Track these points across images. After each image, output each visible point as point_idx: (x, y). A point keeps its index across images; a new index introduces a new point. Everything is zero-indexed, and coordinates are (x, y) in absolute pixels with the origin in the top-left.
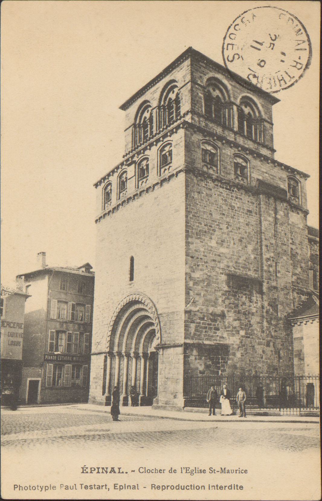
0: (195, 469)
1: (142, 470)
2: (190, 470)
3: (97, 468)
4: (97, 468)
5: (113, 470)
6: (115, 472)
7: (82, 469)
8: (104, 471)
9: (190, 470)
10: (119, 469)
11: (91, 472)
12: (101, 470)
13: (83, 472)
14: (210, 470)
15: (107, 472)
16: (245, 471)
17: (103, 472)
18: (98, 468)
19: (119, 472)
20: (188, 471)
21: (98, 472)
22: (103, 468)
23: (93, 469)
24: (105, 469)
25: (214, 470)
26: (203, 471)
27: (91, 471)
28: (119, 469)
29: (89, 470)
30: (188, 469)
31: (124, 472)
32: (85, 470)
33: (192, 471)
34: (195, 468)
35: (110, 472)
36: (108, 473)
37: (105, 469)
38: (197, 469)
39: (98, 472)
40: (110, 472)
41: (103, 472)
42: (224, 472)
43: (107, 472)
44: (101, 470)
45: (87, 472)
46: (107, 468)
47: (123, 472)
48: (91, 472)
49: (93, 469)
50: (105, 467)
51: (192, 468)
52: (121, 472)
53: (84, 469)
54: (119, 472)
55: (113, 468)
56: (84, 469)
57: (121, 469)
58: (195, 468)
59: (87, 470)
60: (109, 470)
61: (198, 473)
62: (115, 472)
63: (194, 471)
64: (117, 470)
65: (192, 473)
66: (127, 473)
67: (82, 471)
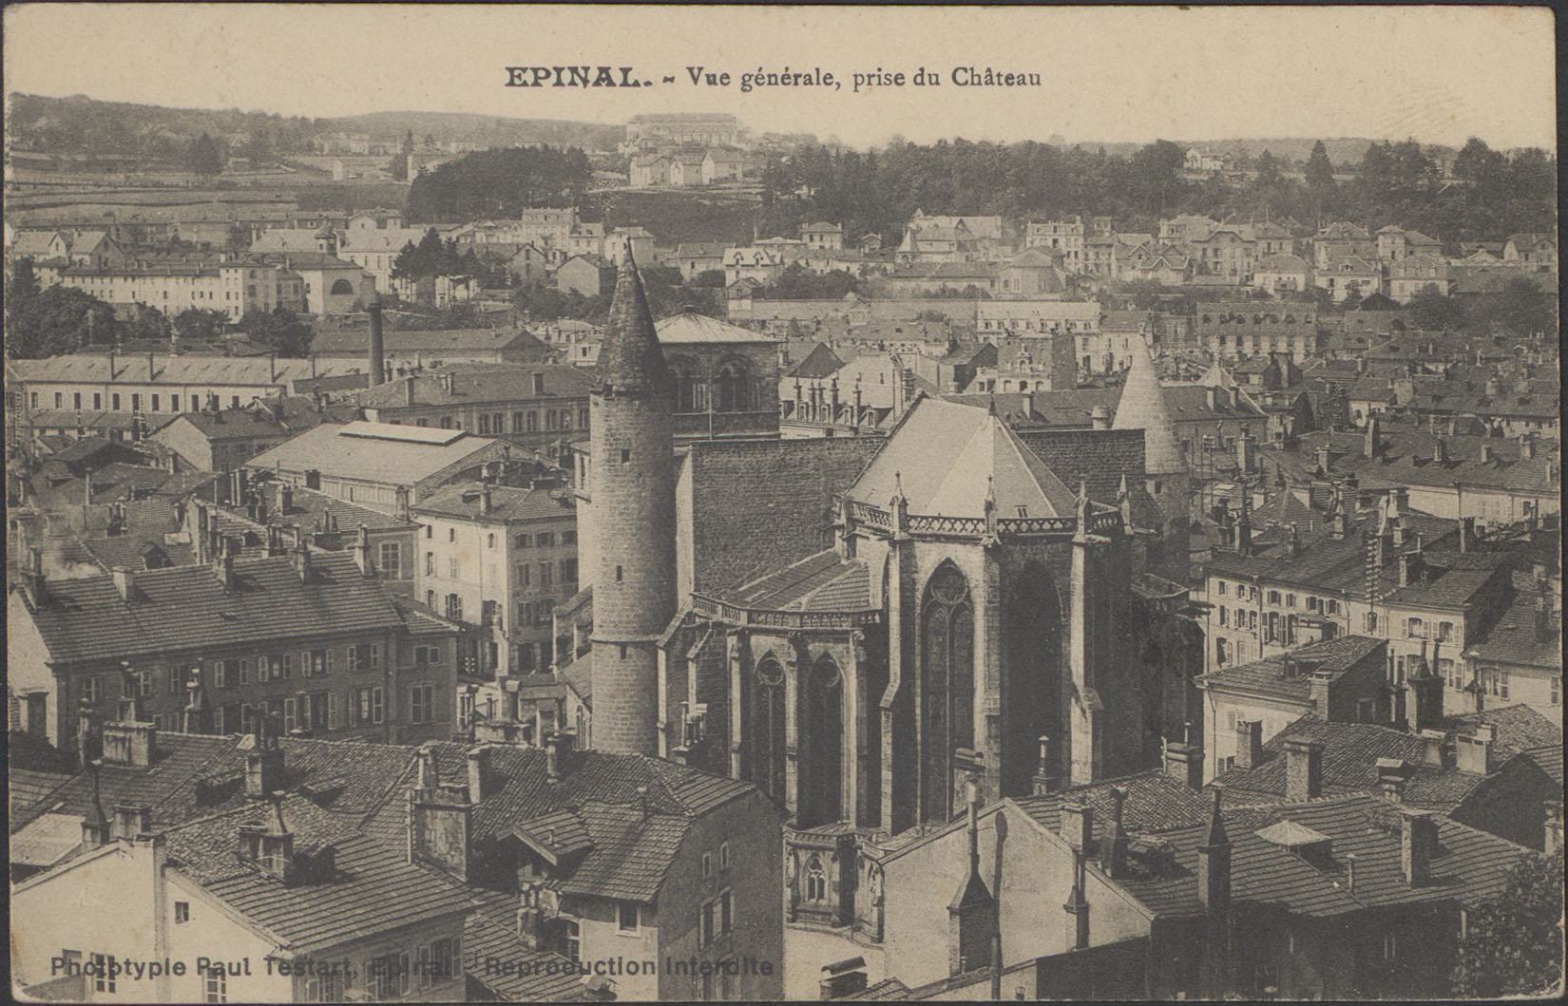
3: (555, 69)
4: (555, 69)
5: (605, 77)
6: (611, 83)
7: (508, 74)
8: (577, 80)
10: (625, 71)
12: (566, 76)
13: (511, 84)
15: (585, 82)
18: (559, 70)
19: (625, 84)
21: (559, 83)
22: (574, 70)
23: (542, 74)
24: (582, 73)
27: (537, 78)
28: (625, 71)
29: (529, 77)
31: (641, 83)
32: (519, 76)
35: (597, 84)
36: (590, 85)
37: (582, 73)
39: (559, 83)
40: (597, 84)
41: (573, 83)
43: (585, 82)
44: (566, 76)
45: (525, 84)
46: (586, 69)
47: (636, 84)
48: (536, 84)
49: (542, 74)
50: (579, 64)
52: (631, 81)
53: (516, 73)
55: (602, 70)
56: (516, 73)
57: (630, 74)
59: (524, 77)
60: (593, 75)
62: (611, 83)
64: (617, 77)
66: (648, 84)
67: (508, 80)
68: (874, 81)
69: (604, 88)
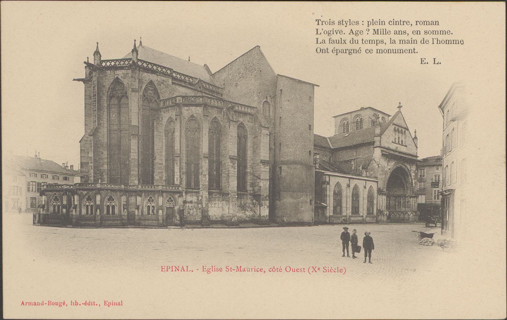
0: (211, 267)
1: (288, 269)
2: (207, 268)
6: (184, 271)
9: (207, 268)
11: (167, 271)
14: (324, 269)
15: (178, 270)
16: (260, 269)
17: (175, 271)
19: (187, 271)
20: (205, 270)
23: (168, 268)
25: (231, 268)
26: (220, 269)
30: (205, 267)
33: (209, 269)
34: (212, 266)
35: (181, 271)
38: (214, 267)
40: (181, 271)
41: (175, 271)
42: (240, 270)
43: (178, 270)
44: (174, 268)
51: (209, 266)
54: (187, 271)
58: (212, 266)
61: (215, 271)
63: (211, 270)
64: (185, 268)
65: (208, 272)
68: (253, 270)
69: (183, 272)
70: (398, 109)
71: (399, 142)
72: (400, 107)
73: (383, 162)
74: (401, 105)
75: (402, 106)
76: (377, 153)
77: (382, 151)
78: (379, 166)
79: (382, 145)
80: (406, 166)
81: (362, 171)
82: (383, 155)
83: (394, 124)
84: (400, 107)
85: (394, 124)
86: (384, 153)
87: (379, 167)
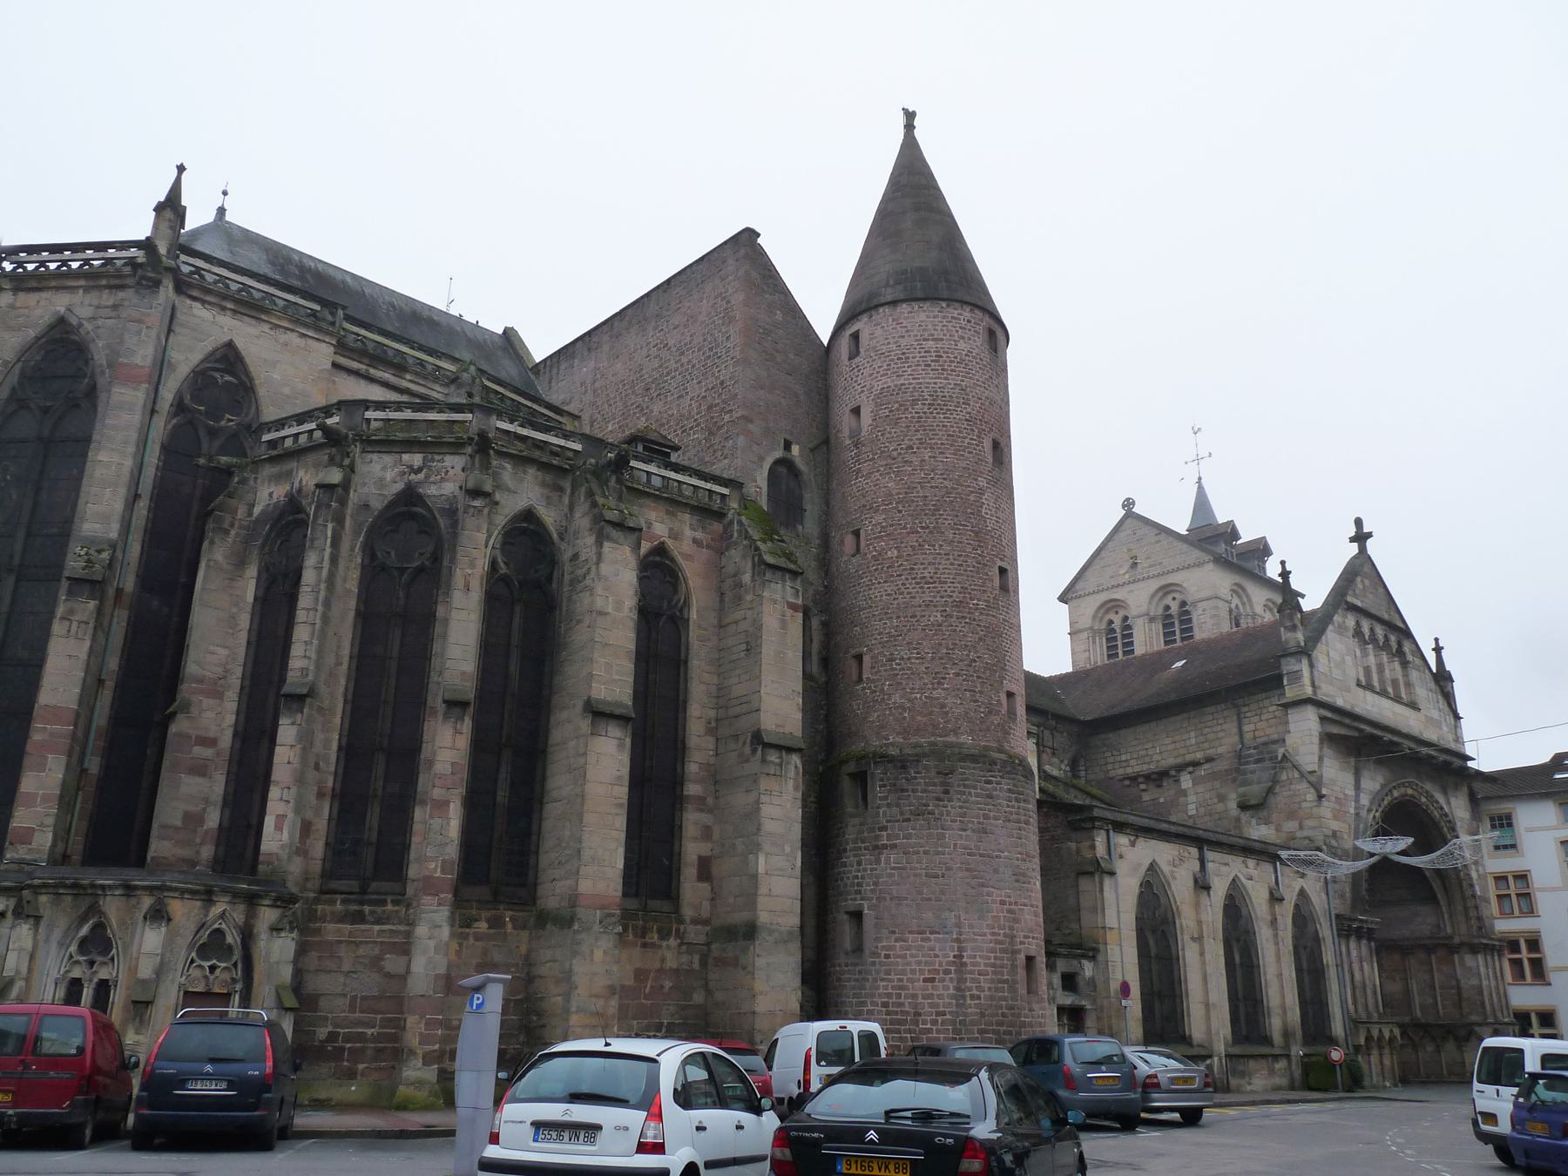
70: (1354, 549)
71: (1382, 681)
72: (1361, 537)
73: (1336, 774)
74: (1366, 530)
75: (1370, 535)
76: (1304, 731)
77: (1323, 719)
78: (1324, 791)
79: (1321, 697)
80: (1430, 796)
81: (1238, 820)
82: (1328, 739)
83: (1353, 608)
84: (1361, 537)
85: (1353, 608)
86: (1335, 730)
87: (1321, 797)
